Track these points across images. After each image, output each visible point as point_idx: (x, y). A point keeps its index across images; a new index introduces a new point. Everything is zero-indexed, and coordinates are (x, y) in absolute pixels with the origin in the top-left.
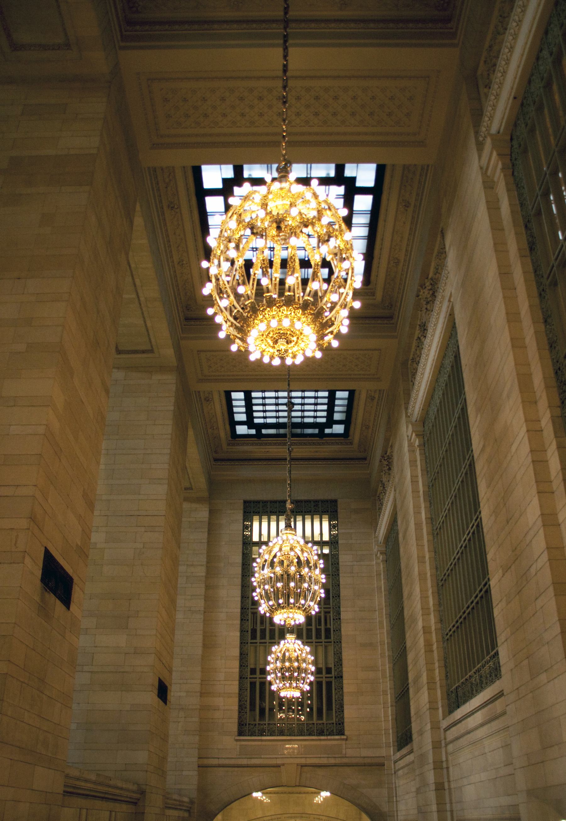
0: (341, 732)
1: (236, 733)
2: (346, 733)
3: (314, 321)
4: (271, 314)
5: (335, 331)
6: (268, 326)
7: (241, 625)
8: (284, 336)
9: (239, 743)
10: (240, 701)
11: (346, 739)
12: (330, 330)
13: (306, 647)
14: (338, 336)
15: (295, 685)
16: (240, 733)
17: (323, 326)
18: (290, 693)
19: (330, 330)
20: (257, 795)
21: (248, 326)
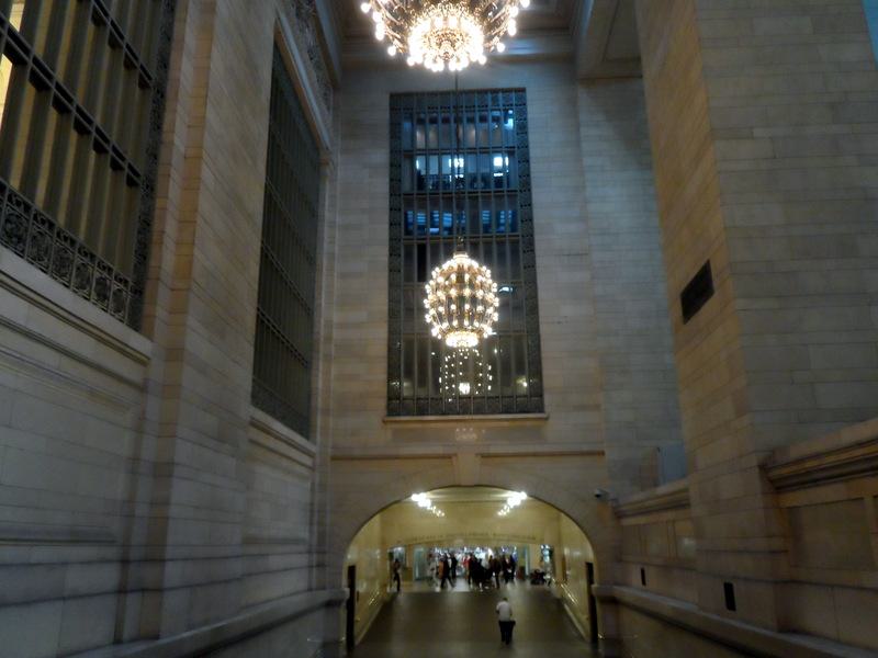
0: (540, 409)
1: (385, 412)
2: (547, 409)
3: (481, 21)
4: (435, 11)
5: (502, 34)
6: (433, 26)
7: (390, 263)
8: (447, 38)
9: (389, 426)
10: (389, 366)
11: (547, 419)
12: (497, 31)
13: (484, 268)
14: (505, 38)
15: (466, 323)
16: (391, 411)
17: (492, 27)
18: (463, 340)
19: (497, 31)
20: (423, 499)
21: (410, 24)
